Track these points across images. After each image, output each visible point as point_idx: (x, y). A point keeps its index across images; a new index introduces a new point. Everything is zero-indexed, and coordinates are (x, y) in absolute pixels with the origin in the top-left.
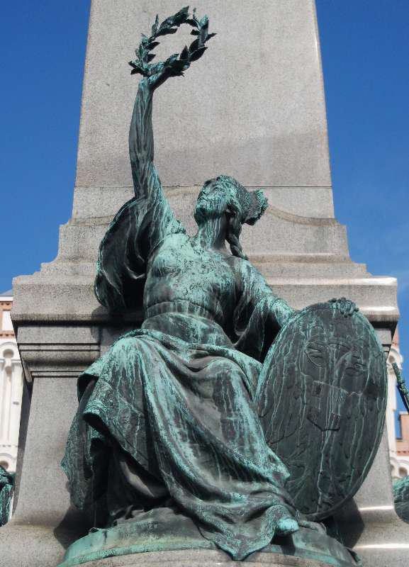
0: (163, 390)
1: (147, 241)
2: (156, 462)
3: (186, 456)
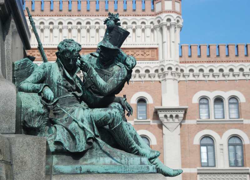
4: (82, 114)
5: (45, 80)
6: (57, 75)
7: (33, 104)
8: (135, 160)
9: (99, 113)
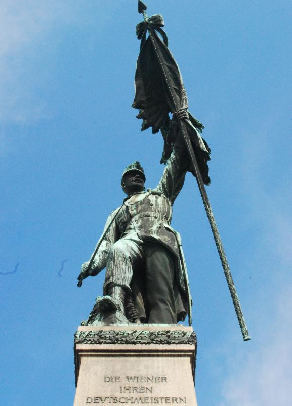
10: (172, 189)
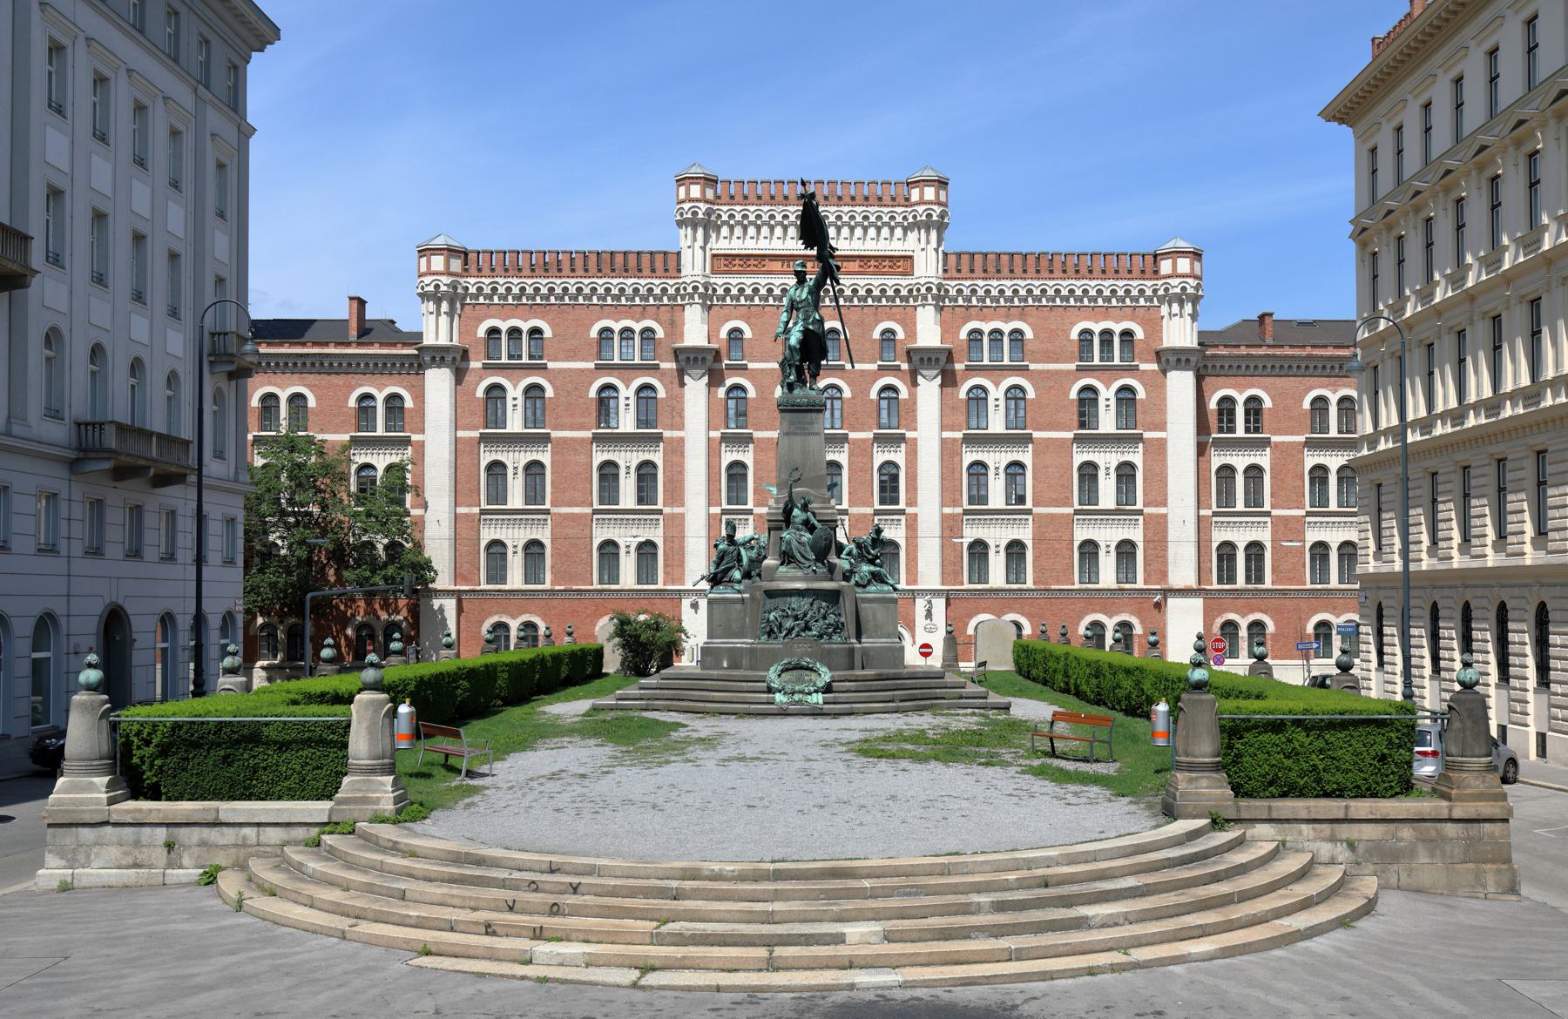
0: (794, 543)
1: (791, 510)
2: (793, 557)
3: (798, 556)
4: (866, 568)
5: (849, 554)
6: (855, 551)
7: (847, 566)
8: (886, 588)
9: (872, 568)
10: (820, 284)
